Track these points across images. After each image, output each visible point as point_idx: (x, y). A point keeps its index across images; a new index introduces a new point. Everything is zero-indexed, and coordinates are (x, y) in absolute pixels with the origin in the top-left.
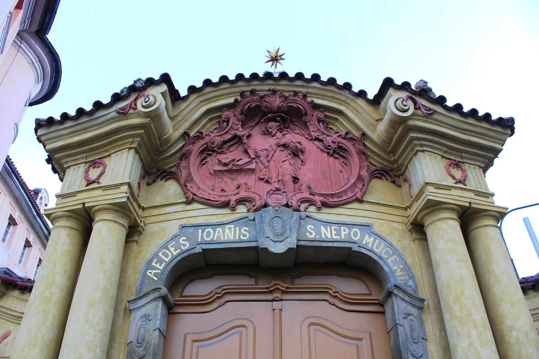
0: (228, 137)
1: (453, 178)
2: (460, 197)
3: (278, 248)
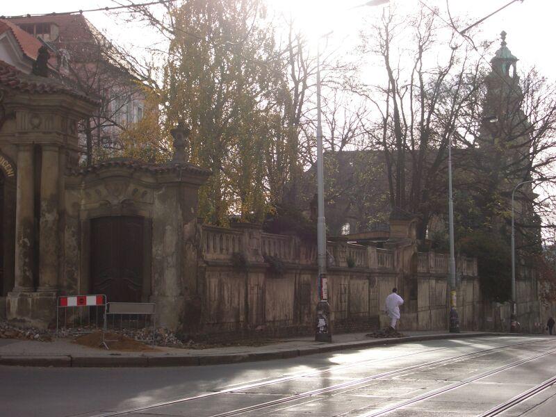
1: (32, 124)
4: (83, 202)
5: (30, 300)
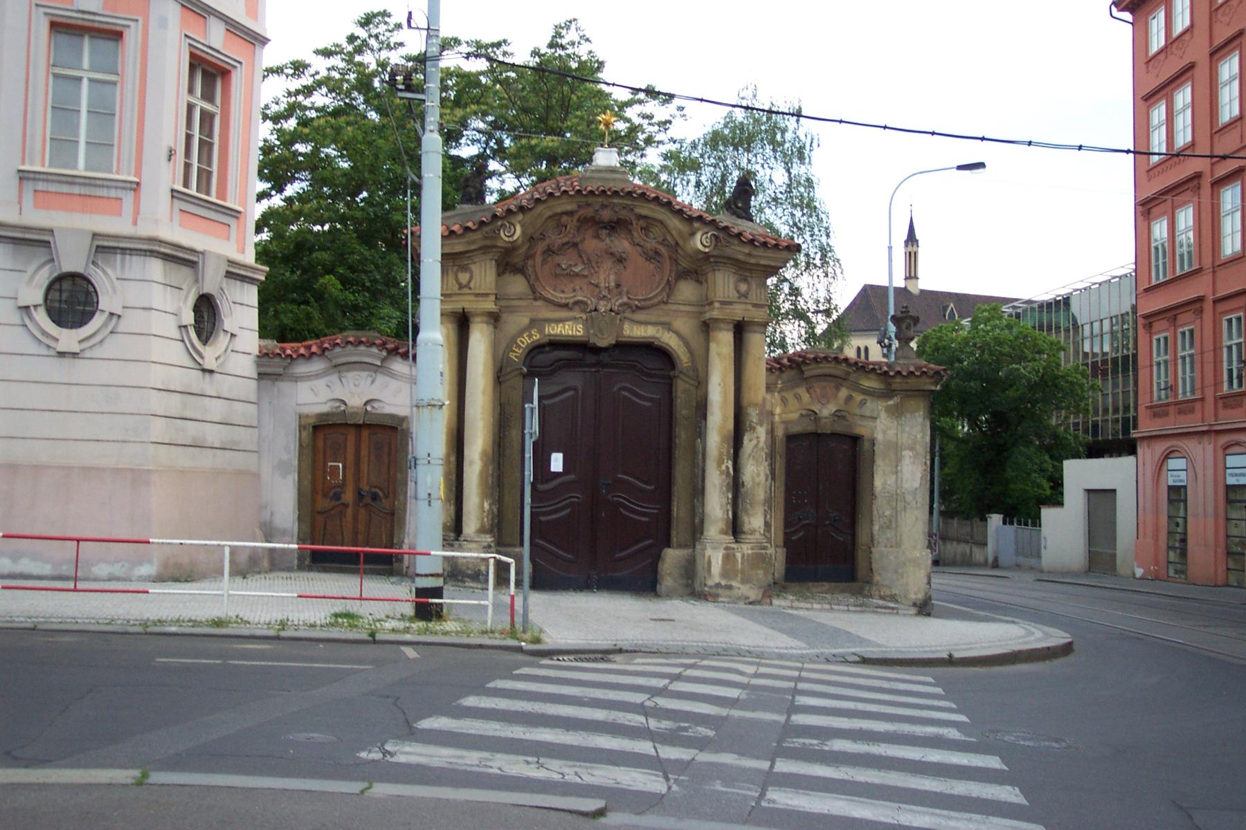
0: (566, 240)
1: (738, 292)
2: (739, 312)
3: (603, 343)
4: (778, 410)
5: (739, 556)
